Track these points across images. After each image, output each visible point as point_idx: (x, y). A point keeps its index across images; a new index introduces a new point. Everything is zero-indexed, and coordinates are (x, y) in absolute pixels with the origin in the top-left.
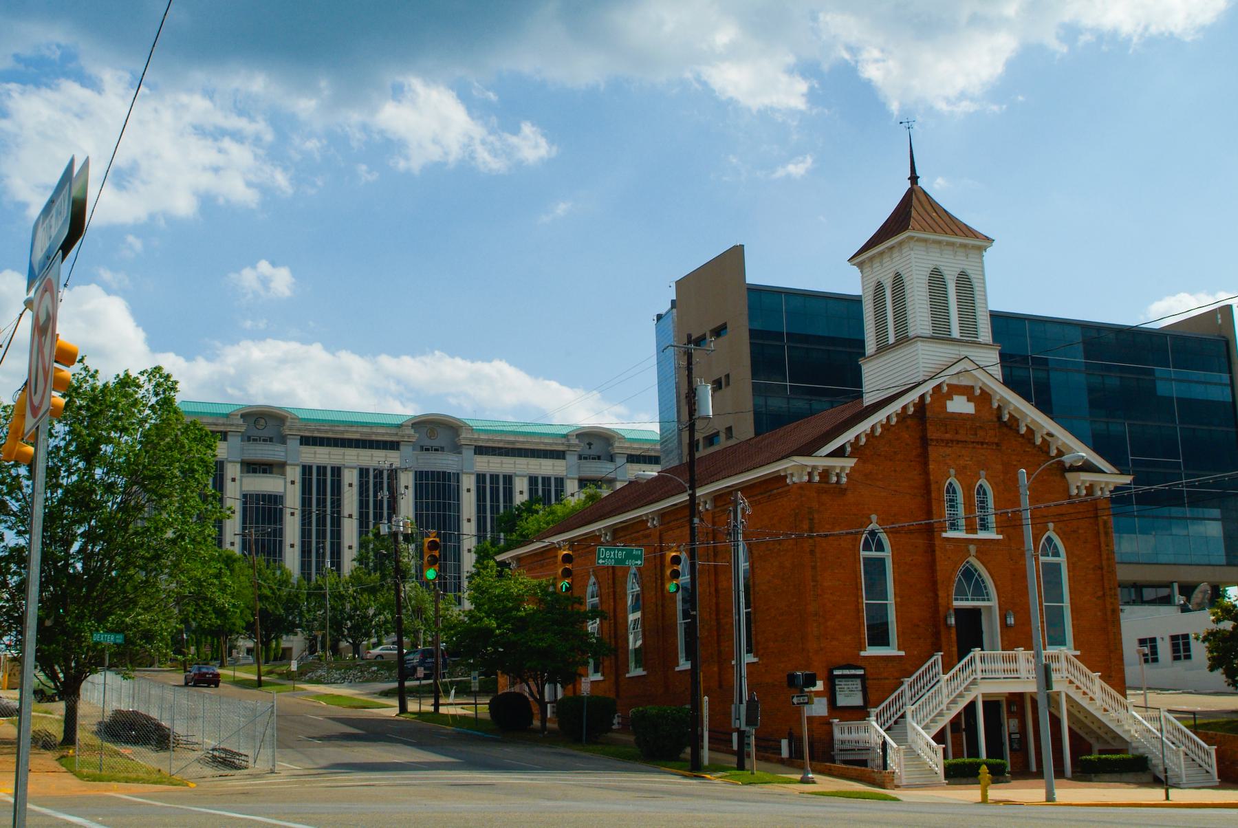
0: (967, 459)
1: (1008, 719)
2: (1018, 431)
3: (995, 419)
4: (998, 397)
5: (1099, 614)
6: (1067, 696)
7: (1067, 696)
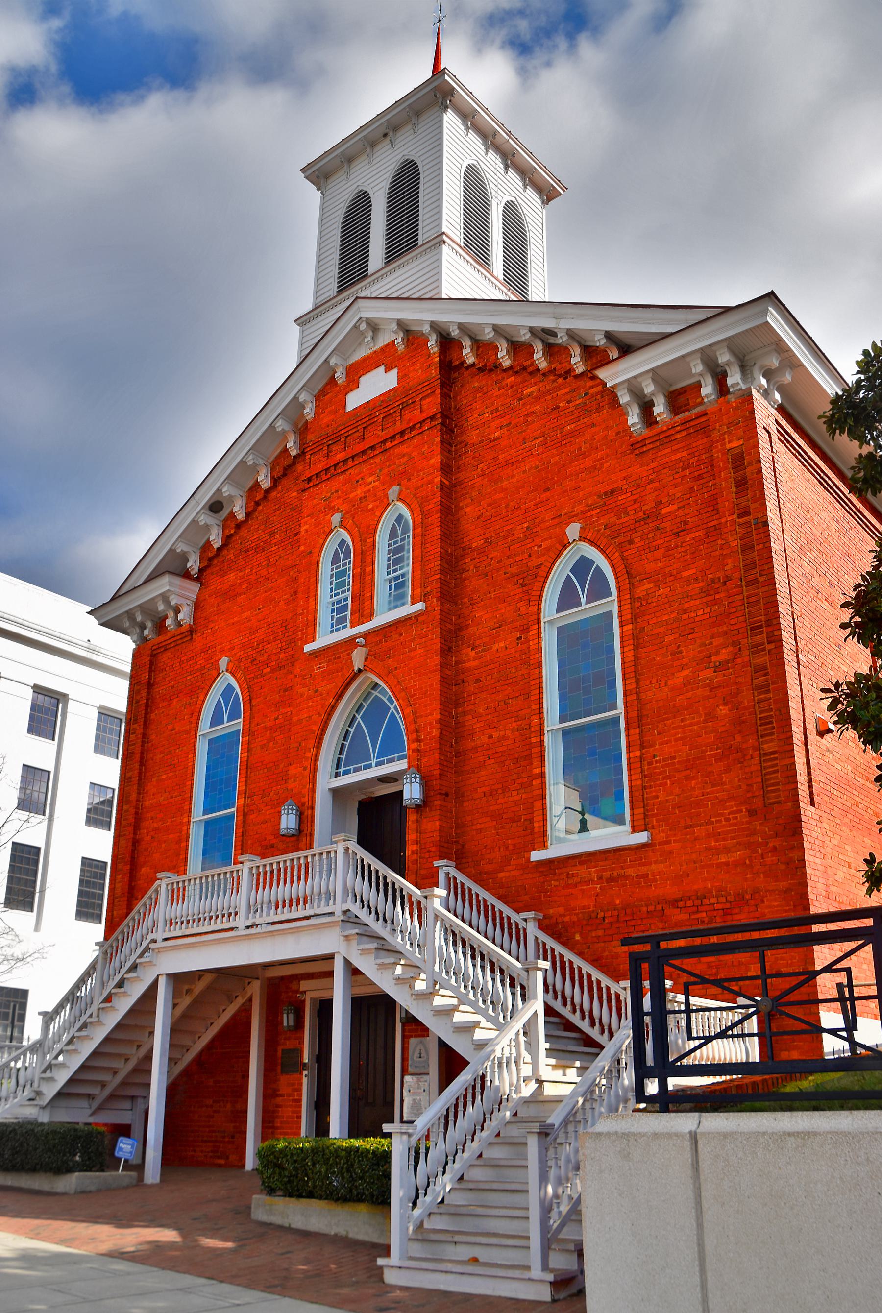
0: (370, 479)
1: (404, 1038)
2: (498, 366)
3: (434, 372)
4: (426, 329)
5: (723, 710)
6: (347, 962)
7: (347, 962)
